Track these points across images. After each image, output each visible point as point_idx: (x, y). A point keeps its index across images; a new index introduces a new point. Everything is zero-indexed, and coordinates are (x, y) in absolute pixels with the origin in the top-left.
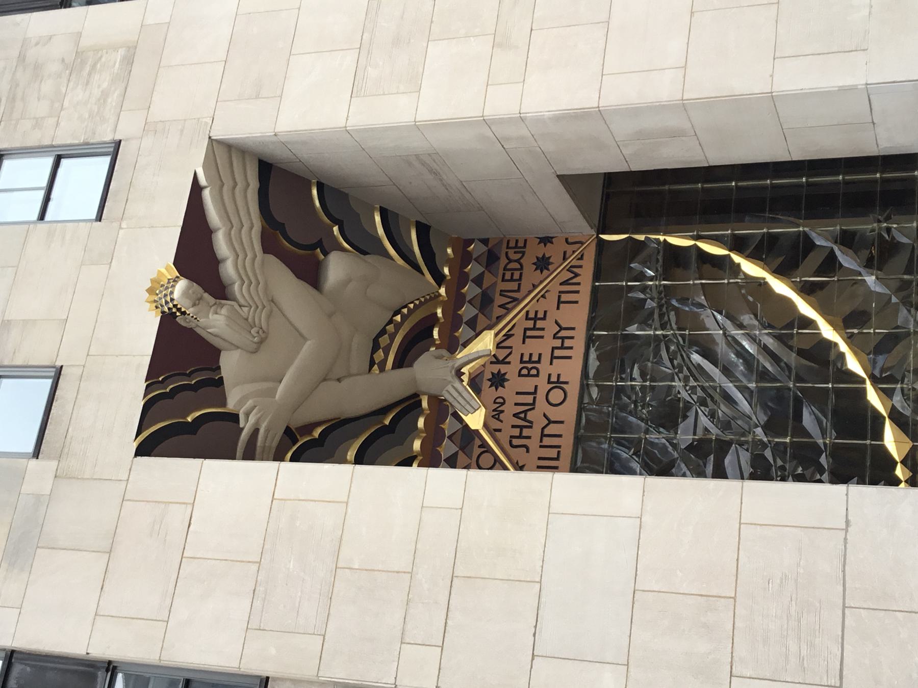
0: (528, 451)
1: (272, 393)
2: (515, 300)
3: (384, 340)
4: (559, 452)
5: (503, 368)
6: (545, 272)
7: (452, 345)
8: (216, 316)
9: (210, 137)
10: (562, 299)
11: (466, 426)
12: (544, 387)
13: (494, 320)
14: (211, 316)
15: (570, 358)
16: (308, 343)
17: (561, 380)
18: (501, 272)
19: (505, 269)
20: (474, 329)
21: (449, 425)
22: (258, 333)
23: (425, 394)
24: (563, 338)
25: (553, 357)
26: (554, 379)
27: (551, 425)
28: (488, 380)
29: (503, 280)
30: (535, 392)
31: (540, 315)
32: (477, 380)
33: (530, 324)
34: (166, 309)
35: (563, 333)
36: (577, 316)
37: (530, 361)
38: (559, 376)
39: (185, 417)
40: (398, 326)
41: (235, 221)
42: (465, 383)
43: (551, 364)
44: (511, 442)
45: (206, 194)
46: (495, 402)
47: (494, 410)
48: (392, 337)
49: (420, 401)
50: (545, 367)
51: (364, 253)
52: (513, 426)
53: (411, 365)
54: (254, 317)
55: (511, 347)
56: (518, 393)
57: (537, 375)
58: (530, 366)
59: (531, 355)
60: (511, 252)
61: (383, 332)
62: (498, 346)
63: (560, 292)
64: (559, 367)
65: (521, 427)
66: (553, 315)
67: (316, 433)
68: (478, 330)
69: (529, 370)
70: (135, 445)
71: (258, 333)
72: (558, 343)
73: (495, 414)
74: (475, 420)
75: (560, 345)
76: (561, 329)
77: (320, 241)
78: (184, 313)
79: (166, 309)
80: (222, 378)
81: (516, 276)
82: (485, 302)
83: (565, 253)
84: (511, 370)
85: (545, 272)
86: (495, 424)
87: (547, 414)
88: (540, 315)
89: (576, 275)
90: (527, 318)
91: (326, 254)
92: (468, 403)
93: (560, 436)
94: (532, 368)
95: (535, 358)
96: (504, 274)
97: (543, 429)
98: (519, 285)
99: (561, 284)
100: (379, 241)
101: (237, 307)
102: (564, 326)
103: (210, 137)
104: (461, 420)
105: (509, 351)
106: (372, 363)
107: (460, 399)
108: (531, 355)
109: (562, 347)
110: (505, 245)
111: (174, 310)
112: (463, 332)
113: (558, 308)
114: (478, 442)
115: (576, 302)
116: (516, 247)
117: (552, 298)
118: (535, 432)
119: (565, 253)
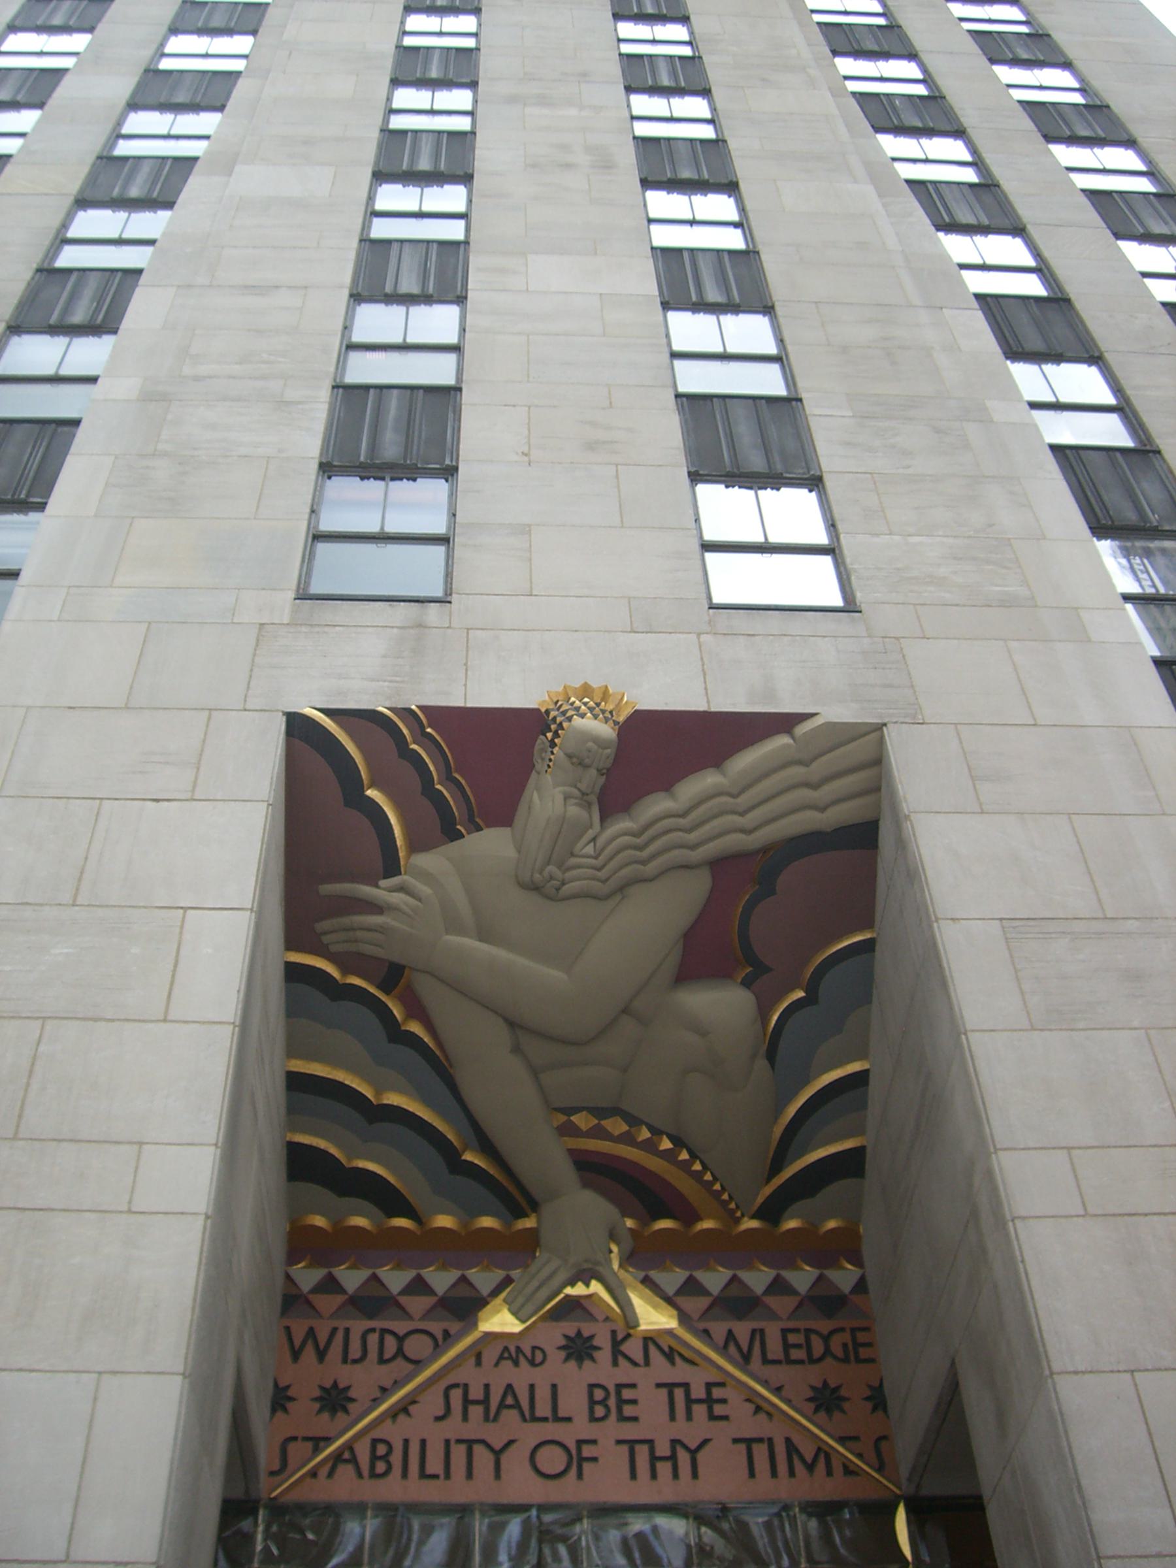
0: (438, 1419)
1: (454, 925)
2: (746, 1358)
4: (436, 1476)
5: (604, 1355)
6: (812, 1406)
8: (562, 797)
9: (885, 725)
10: (755, 1446)
12: (568, 1434)
13: (702, 1325)
14: (558, 793)
15: (633, 1475)
19: (808, 1331)
20: (679, 1292)
22: (551, 878)
23: (539, 1222)
24: (673, 1458)
25: (632, 1444)
26: (587, 1451)
28: (579, 1335)
29: (785, 1332)
31: (718, 1409)
33: (698, 1392)
34: (553, 714)
35: (683, 1457)
37: (621, 1402)
38: (594, 1459)
40: (649, 1146)
41: (744, 800)
42: (569, 1291)
43: (619, 1442)
44: (456, 1386)
45: (783, 740)
46: (534, 1348)
47: (518, 1349)
48: (627, 1139)
49: (526, 1215)
50: (612, 1429)
52: (487, 1386)
53: (586, 1184)
54: (579, 866)
55: (647, 1363)
56: (554, 1386)
57: (593, 1419)
59: (634, 1402)
60: (846, 1337)
61: (633, 1121)
62: (649, 1340)
63: (770, 1440)
65: (485, 1402)
66: (722, 1434)
67: (415, 1028)
69: (604, 1402)
70: (308, 711)
71: (551, 878)
72: (663, 1449)
75: (658, 1454)
76: (694, 1453)
77: (768, 970)
78: (553, 744)
79: (553, 714)
81: (795, 1354)
82: (737, 1303)
83: (856, 1438)
84: (602, 1370)
85: (812, 1406)
87: (514, 1447)
88: (718, 1409)
89: (810, 1467)
90: (709, 1386)
91: (747, 983)
92: (528, 1300)
93: (470, 1475)
94: (607, 1407)
95: (628, 1410)
96: (796, 1330)
97: (483, 1442)
98: (778, 1362)
99: (788, 1440)
100: (806, 1082)
101: (590, 833)
102: (701, 1456)
104: (495, 1293)
107: (535, 1283)
108: (634, 1402)
109: (654, 1459)
110: (856, 1324)
111: (553, 727)
113: (736, 1441)
114: (454, 1327)
115: (752, 1474)
116: (857, 1345)
118: (475, 1427)
119: (856, 1438)
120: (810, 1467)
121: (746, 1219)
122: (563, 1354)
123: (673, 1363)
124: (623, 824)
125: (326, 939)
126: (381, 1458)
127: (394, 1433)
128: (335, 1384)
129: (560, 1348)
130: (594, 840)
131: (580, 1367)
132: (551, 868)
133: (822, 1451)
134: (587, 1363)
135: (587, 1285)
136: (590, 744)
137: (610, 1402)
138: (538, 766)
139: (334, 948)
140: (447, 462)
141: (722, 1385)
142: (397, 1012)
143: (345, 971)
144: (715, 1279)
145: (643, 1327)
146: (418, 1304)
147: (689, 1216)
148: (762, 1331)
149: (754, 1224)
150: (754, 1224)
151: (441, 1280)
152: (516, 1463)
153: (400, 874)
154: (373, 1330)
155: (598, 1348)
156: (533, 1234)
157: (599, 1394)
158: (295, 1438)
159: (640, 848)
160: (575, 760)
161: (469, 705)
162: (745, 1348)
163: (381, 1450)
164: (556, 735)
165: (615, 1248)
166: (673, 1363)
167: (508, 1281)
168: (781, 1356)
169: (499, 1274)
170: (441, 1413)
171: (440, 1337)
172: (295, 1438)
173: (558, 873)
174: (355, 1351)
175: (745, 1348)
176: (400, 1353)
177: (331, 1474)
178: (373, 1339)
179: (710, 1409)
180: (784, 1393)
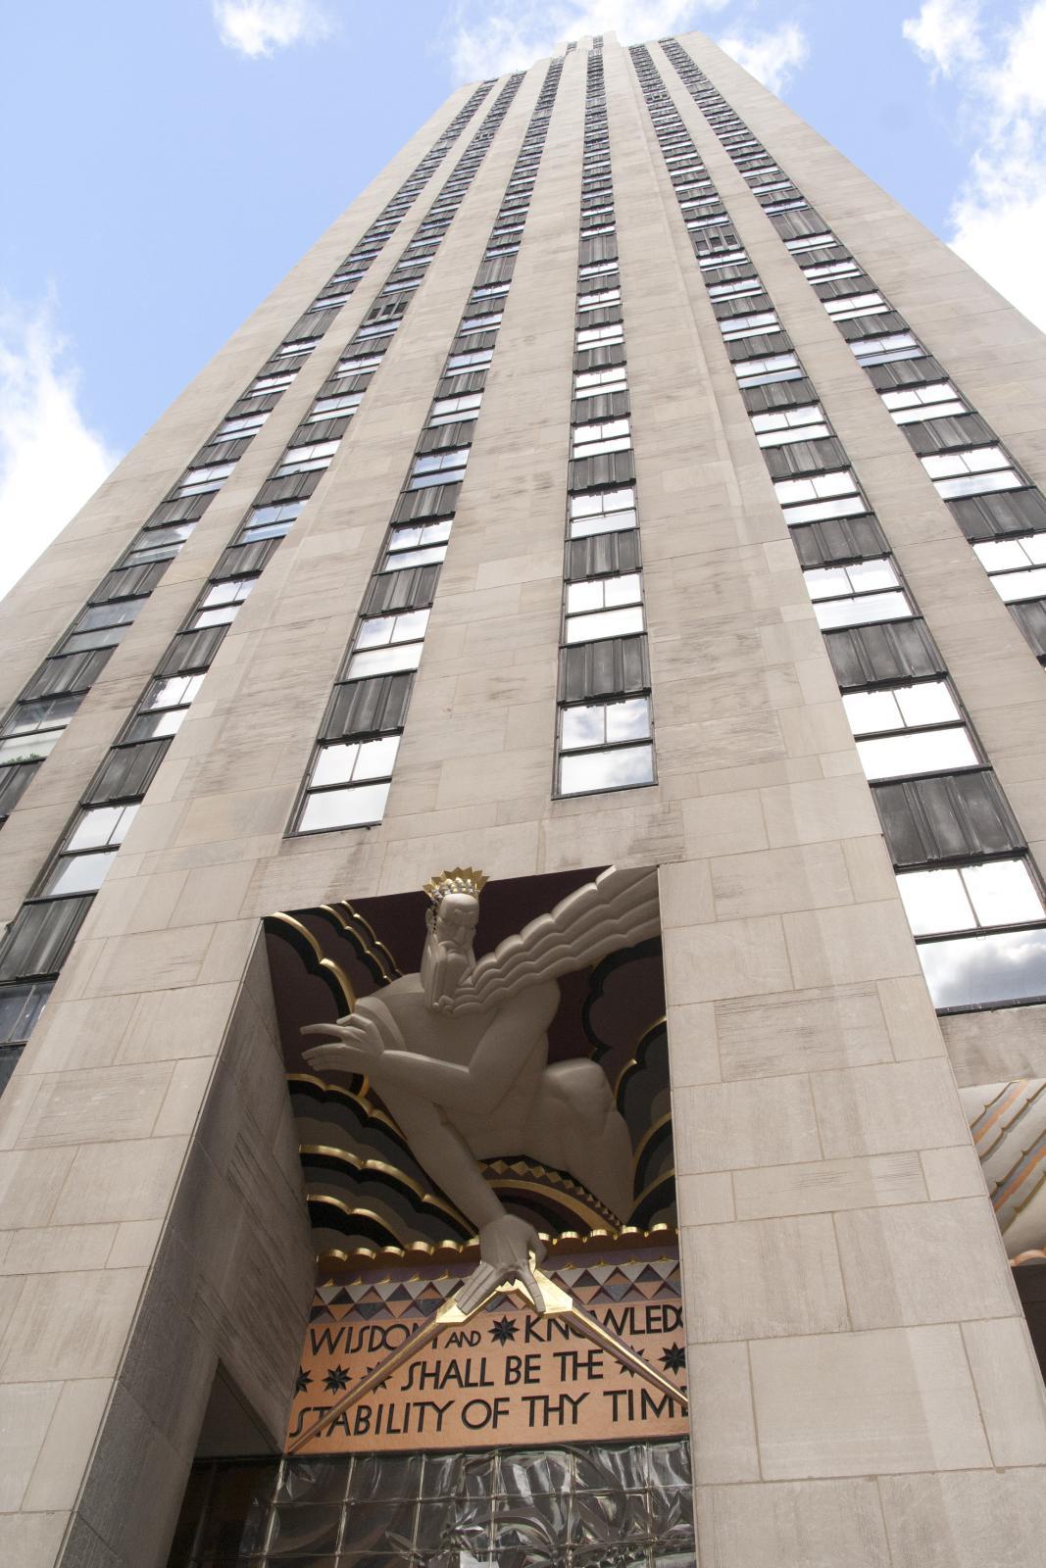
0: (404, 1389)
2: (619, 1330)
3: (518, 1168)
4: (398, 1431)
5: (519, 1335)
6: (663, 1364)
7: (552, 1260)
8: (443, 949)
11: (442, 1302)
12: (488, 1394)
13: (589, 1308)
16: (466, 1070)
17: (500, 1417)
18: (661, 1302)
19: (665, 1307)
20: (577, 1284)
21: (443, 1283)
24: (560, 1409)
25: (532, 1399)
26: (502, 1406)
27: (436, 1415)
29: (648, 1309)
30: (483, 1383)
31: (596, 1370)
32: (507, 1303)
33: (583, 1358)
35: (568, 1407)
36: (595, 1422)
37: (528, 1368)
38: (506, 1412)
39: (325, 956)
40: (544, 1181)
42: (500, 1289)
44: (418, 1364)
45: (592, 887)
46: (473, 1332)
47: (462, 1334)
48: (528, 1177)
49: (472, 1237)
50: (523, 1389)
51: (620, 1108)
53: (509, 1212)
55: (549, 1339)
56: (484, 1360)
57: (508, 1382)
58: (522, 1370)
59: (538, 1368)
62: (552, 1320)
63: (631, 1392)
64: (518, 1410)
65: (436, 1375)
66: (597, 1388)
67: (377, 1114)
68: (576, 1290)
69: (516, 1370)
72: (554, 1403)
73: (459, 1337)
74: (452, 1314)
75: (551, 1406)
76: (575, 1404)
78: (435, 914)
80: (386, 983)
81: (655, 1325)
84: (518, 1346)
85: (663, 1364)
86: (443, 1338)
87: (453, 1405)
88: (596, 1370)
89: (658, 1412)
90: (591, 1353)
91: (596, 1059)
93: (420, 1429)
95: (533, 1375)
97: (432, 1404)
98: (642, 1332)
99: (644, 1391)
100: (649, 1125)
102: (578, 1406)
103: (658, 866)
105: (545, 1337)
106: (489, 1161)
107: (476, 1285)
108: (538, 1368)
109: (547, 1410)
112: (571, 1275)
113: (606, 1393)
114: (421, 1320)
115: (615, 1418)
117: (626, 1381)
118: (429, 1393)
120: (658, 1412)
121: (624, 1226)
122: (492, 1336)
123: (567, 1337)
124: (491, 959)
125: (310, 1063)
126: (361, 1420)
127: (372, 1400)
128: (339, 1368)
129: (490, 1331)
130: (471, 974)
131: (503, 1344)
133: (669, 1398)
134: (508, 1341)
135: (512, 1284)
136: (457, 910)
137: (521, 1370)
139: (316, 1069)
140: (399, 725)
141: (600, 1351)
142: (366, 1108)
143: (327, 1083)
144: (601, 1273)
145: (548, 1312)
146: (398, 1307)
147: (584, 1229)
148: (632, 1309)
149: (633, 1230)
150: (633, 1230)
151: (415, 1286)
152: (452, 1416)
153: (348, 1013)
154: (368, 1327)
155: (516, 1330)
156: (477, 1248)
157: (514, 1364)
158: (308, 1409)
159: (501, 975)
161: (379, 895)
162: (619, 1324)
163: (364, 1413)
164: (436, 905)
165: (532, 1255)
166: (567, 1337)
167: (461, 1284)
168: (644, 1327)
169: (456, 1280)
170: (406, 1384)
171: (410, 1327)
172: (308, 1409)
174: (354, 1345)
175: (619, 1324)
176: (384, 1343)
177: (329, 1434)
178: (367, 1334)
179: (590, 1370)
180: (644, 1355)
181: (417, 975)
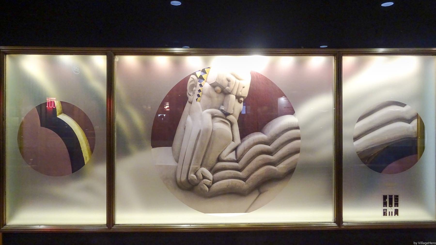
8: (209, 117)
14: (206, 114)
71: (204, 177)
101: (233, 145)
132: (205, 171)
138: (190, 98)
160: (218, 88)
173: (209, 175)
181: (169, 149)
